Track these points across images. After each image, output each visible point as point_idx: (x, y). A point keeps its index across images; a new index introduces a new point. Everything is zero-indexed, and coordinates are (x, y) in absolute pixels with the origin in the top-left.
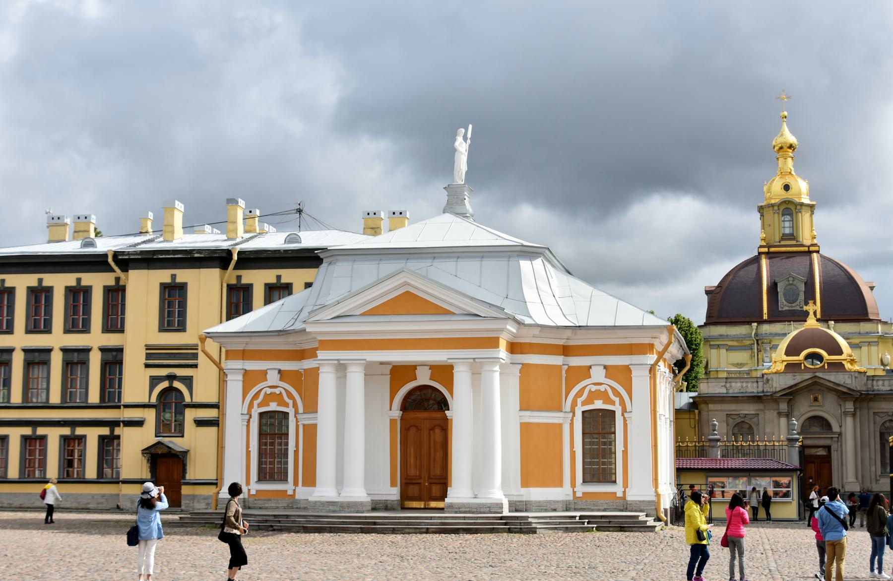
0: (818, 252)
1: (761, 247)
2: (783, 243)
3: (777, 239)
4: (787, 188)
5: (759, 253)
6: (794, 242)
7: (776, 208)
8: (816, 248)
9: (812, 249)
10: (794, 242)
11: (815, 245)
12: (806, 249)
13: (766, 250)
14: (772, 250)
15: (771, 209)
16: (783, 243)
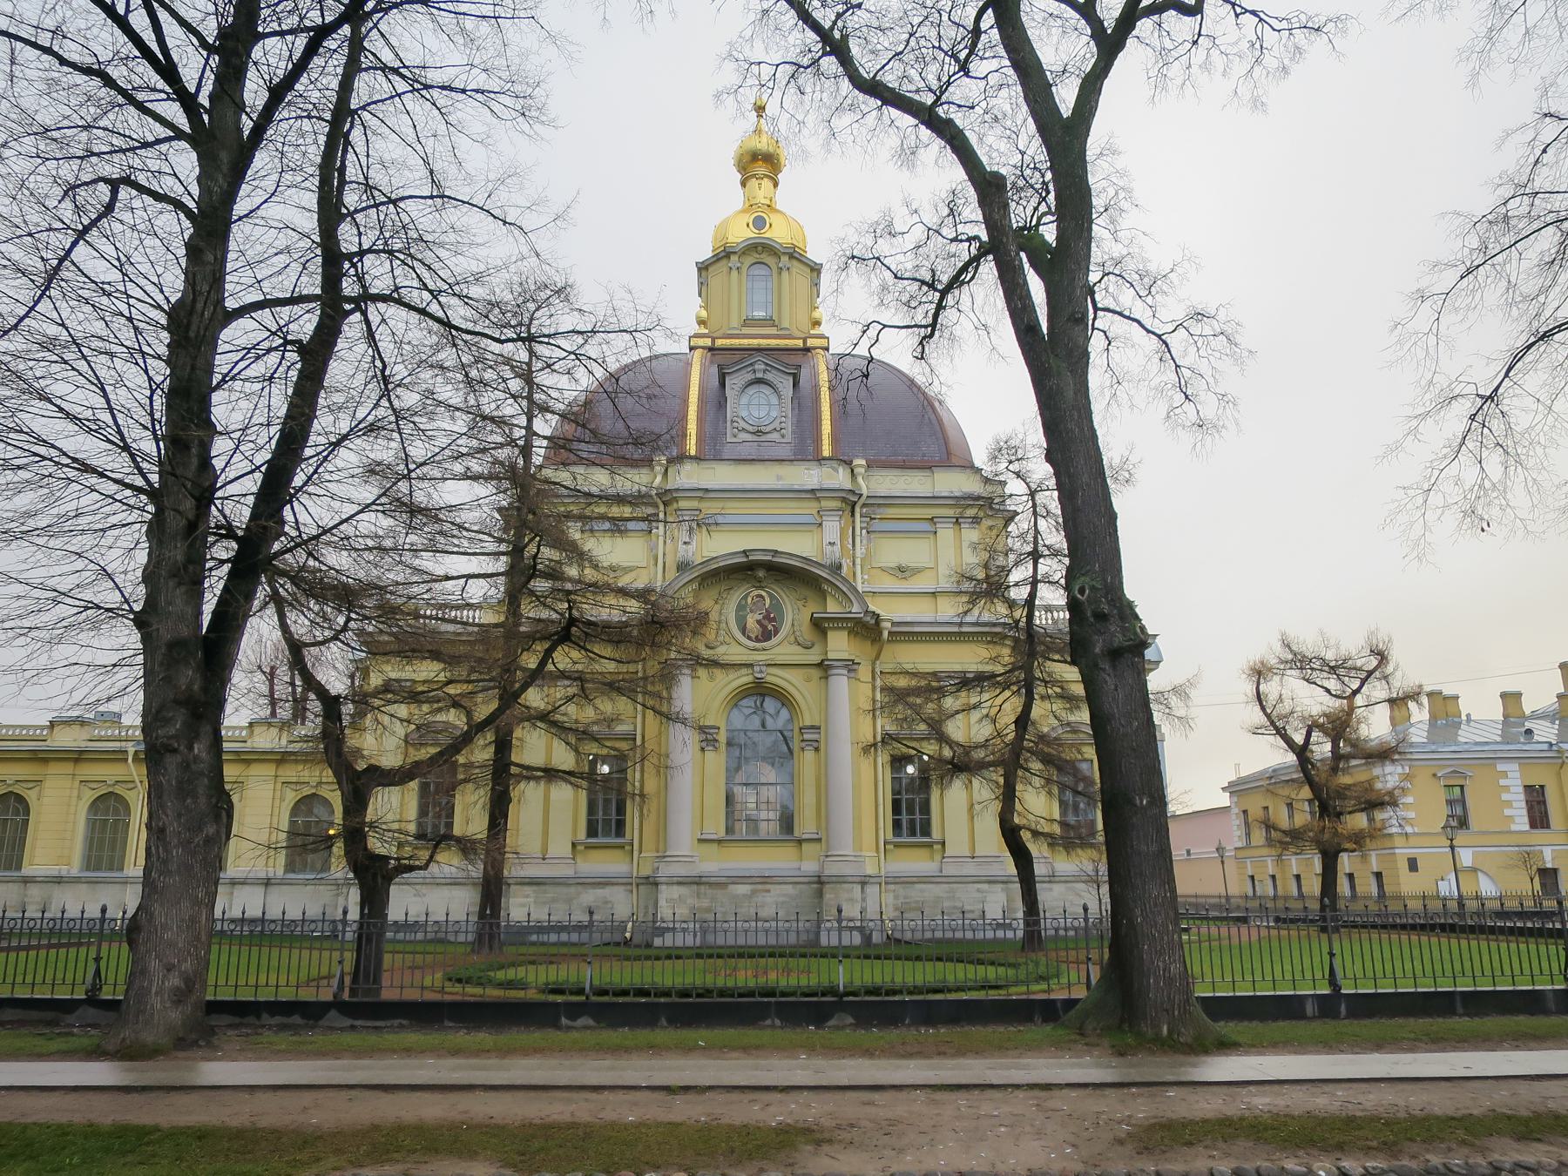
0: (827, 349)
1: (696, 336)
2: (746, 331)
3: (735, 322)
4: (759, 223)
5: (691, 349)
6: (773, 331)
7: (734, 258)
8: (823, 342)
9: (810, 342)
10: (773, 331)
11: (822, 337)
12: (800, 343)
13: (708, 342)
14: (719, 343)
15: (724, 261)
16: (746, 331)
